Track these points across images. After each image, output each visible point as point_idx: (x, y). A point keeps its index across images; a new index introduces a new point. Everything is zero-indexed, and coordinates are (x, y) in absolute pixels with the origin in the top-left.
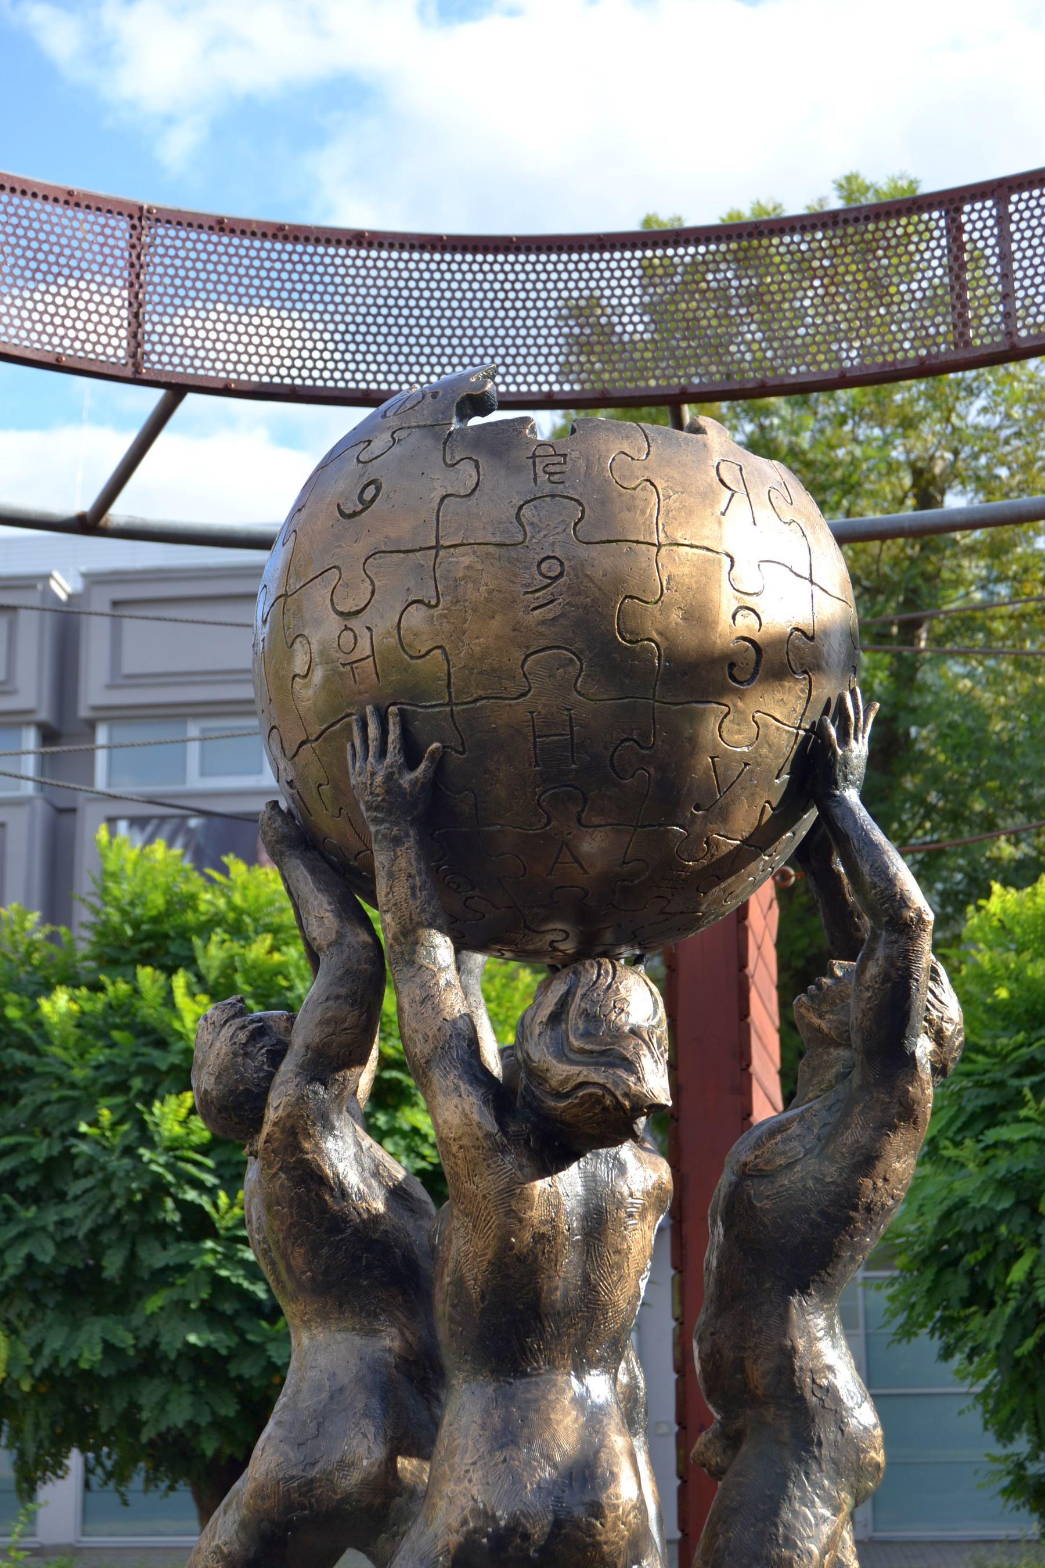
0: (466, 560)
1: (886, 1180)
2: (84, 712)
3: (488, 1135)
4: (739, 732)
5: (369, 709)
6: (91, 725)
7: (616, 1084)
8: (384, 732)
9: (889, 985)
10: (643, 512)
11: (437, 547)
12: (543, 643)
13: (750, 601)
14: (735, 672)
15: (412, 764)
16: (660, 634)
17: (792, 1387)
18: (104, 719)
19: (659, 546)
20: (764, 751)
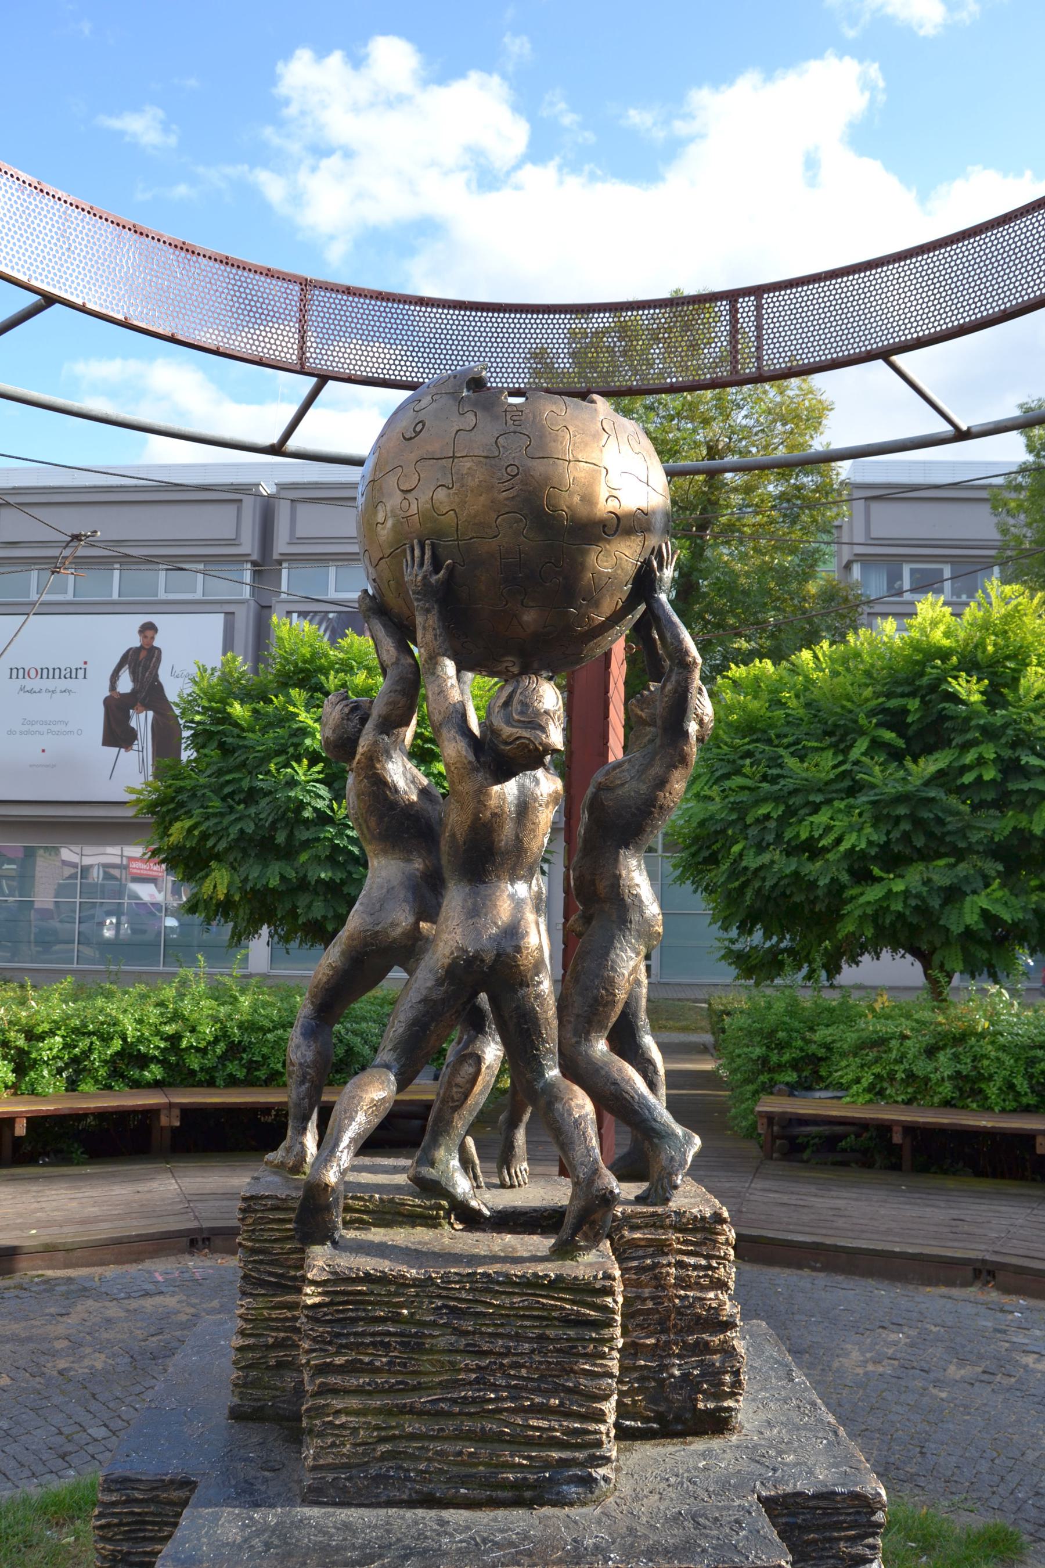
0: (468, 465)
2: (276, 556)
3: (470, 762)
5: (415, 541)
6: (280, 563)
7: (536, 738)
8: (423, 554)
10: (562, 443)
11: (453, 457)
12: (507, 509)
13: (615, 493)
15: (437, 572)
16: (568, 508)
17: (618, 894)
18: (286, 560)
19: (570, 461)
20: (619, 572)
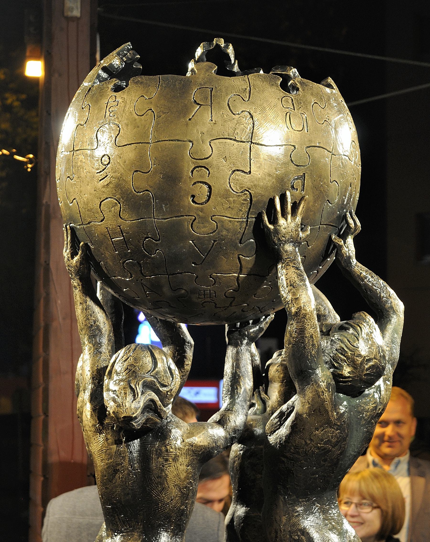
1: (311, 440)
4: (204, 227)
9: (291, 346)
13: (201, 163)
14: (195, 199)
20: (224, 233)
